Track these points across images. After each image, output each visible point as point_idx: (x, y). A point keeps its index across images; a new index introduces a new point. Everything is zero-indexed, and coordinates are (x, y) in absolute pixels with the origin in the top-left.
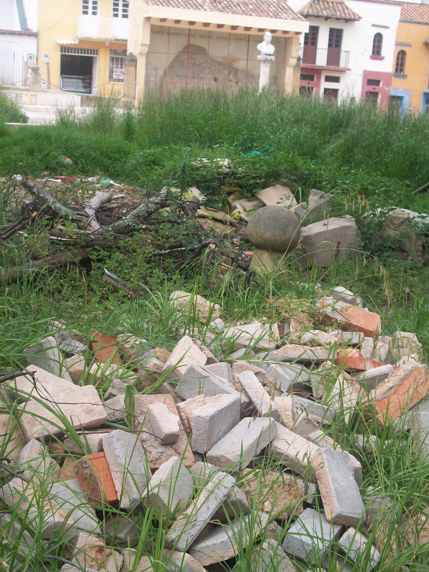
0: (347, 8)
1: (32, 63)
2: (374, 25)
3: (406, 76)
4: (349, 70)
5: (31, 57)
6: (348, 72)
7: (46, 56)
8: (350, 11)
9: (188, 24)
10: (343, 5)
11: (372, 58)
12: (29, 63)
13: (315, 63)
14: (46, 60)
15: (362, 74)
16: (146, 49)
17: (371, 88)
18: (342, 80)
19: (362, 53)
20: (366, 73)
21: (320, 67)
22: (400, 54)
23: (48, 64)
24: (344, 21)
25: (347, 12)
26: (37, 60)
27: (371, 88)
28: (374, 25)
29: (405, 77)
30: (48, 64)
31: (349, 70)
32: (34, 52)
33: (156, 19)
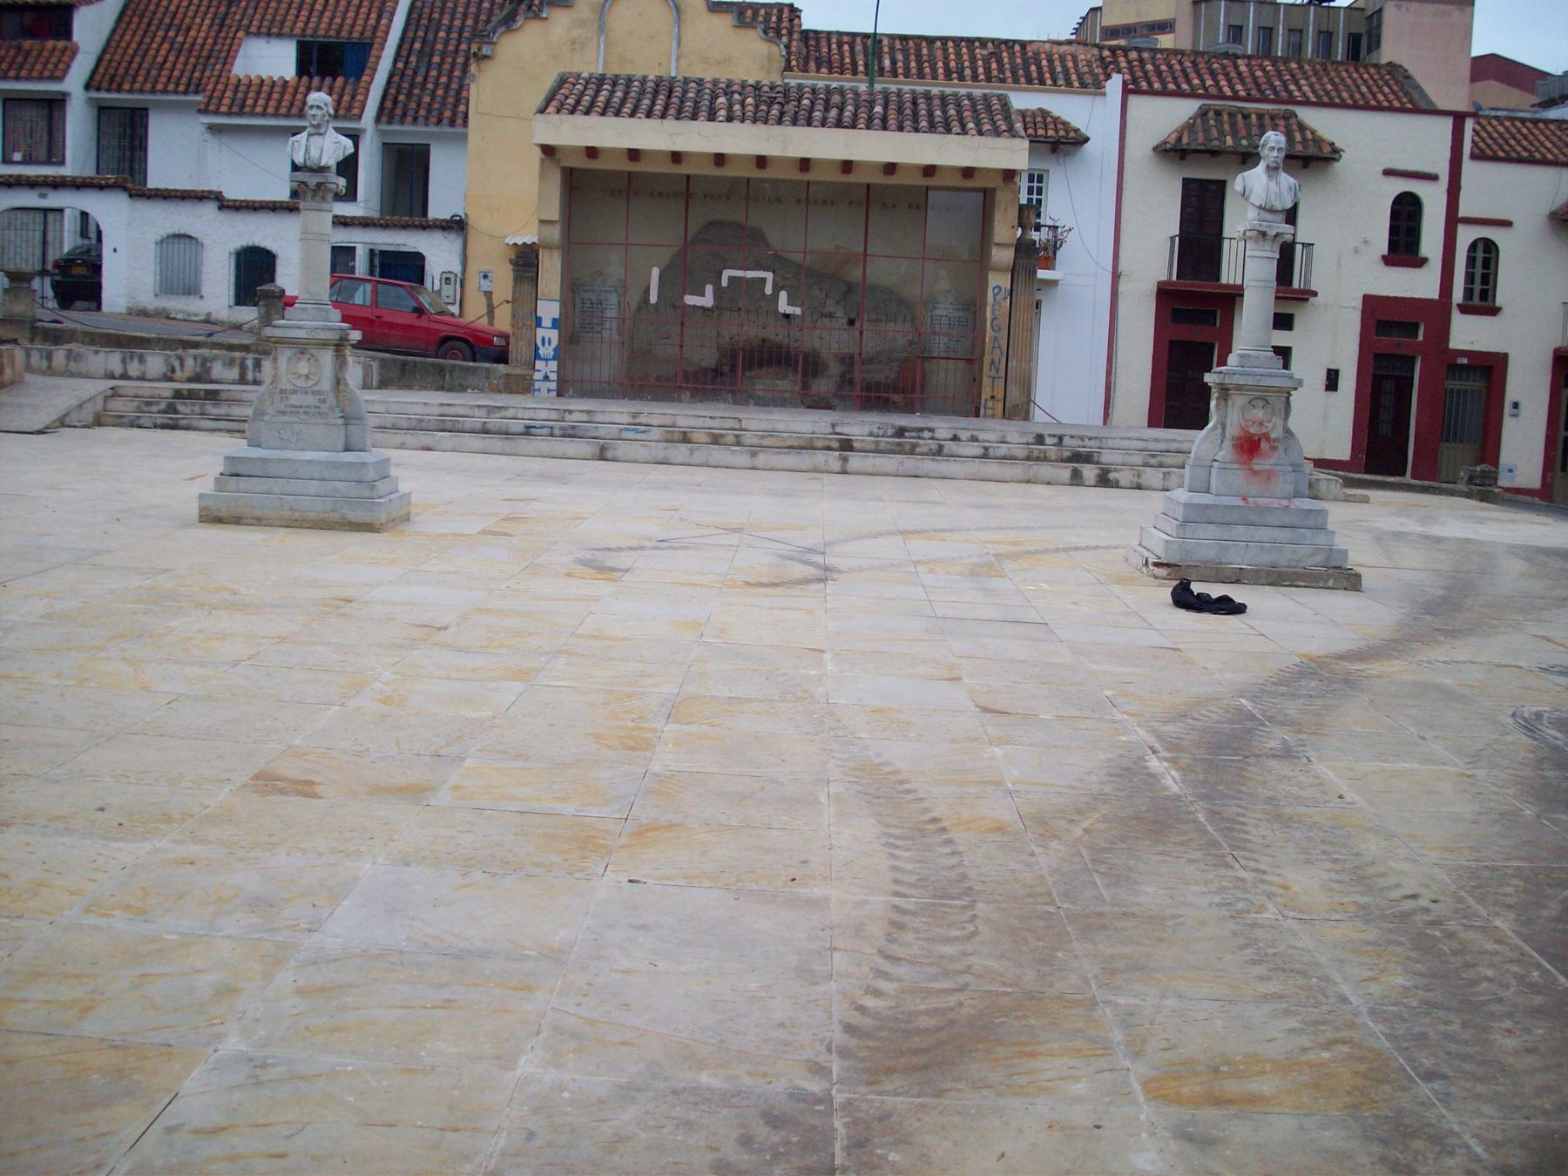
0: (1302, 127)
1: (451, 293)
2: (1388, 173)
3: (1499, 309)
4: (1315, 294)
5: (448, 279)
6: (1312, 299)
7: (485, 277)
8: (1309, 136)
9: (626, 158)
10: (1293, 121)
11: (1388, 261)
12: (444, 293)
13: (1218, 279)
14: (486, 285)
15: (1359, 304)
16: (555, 233)
17: (1385, 343)
18: (1297, 323)
19: (1356, 251)
20: (1371, 304)
21: (1227, 286)
22: (1480, 248)
23: (488, 294)
24: (1300, 162)
25: (1298, 137)
26: (462, 286)
27: (1385, 343)
28: (1388, 173)
29: (1494, 311)
30: (488, 294)
31: (1315, 294)
32: (457, 269)
33: (573, 150)
